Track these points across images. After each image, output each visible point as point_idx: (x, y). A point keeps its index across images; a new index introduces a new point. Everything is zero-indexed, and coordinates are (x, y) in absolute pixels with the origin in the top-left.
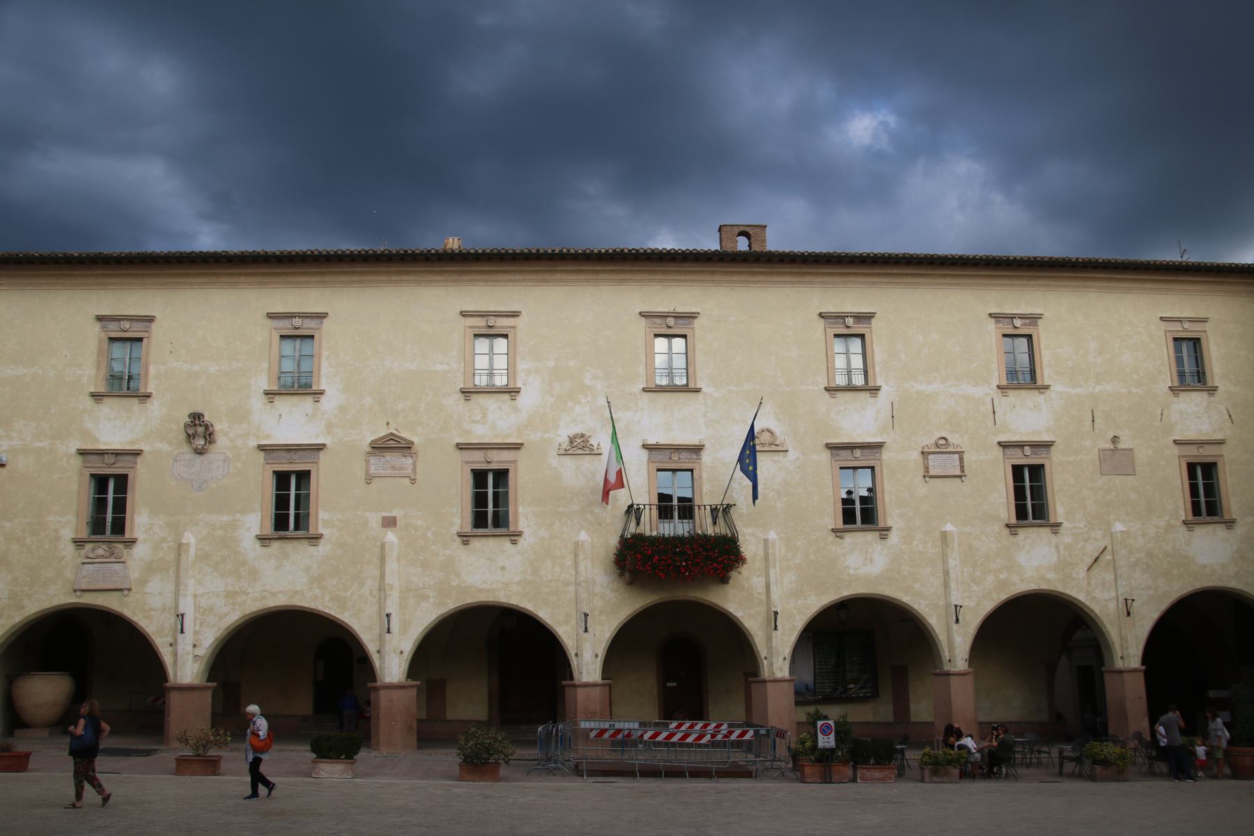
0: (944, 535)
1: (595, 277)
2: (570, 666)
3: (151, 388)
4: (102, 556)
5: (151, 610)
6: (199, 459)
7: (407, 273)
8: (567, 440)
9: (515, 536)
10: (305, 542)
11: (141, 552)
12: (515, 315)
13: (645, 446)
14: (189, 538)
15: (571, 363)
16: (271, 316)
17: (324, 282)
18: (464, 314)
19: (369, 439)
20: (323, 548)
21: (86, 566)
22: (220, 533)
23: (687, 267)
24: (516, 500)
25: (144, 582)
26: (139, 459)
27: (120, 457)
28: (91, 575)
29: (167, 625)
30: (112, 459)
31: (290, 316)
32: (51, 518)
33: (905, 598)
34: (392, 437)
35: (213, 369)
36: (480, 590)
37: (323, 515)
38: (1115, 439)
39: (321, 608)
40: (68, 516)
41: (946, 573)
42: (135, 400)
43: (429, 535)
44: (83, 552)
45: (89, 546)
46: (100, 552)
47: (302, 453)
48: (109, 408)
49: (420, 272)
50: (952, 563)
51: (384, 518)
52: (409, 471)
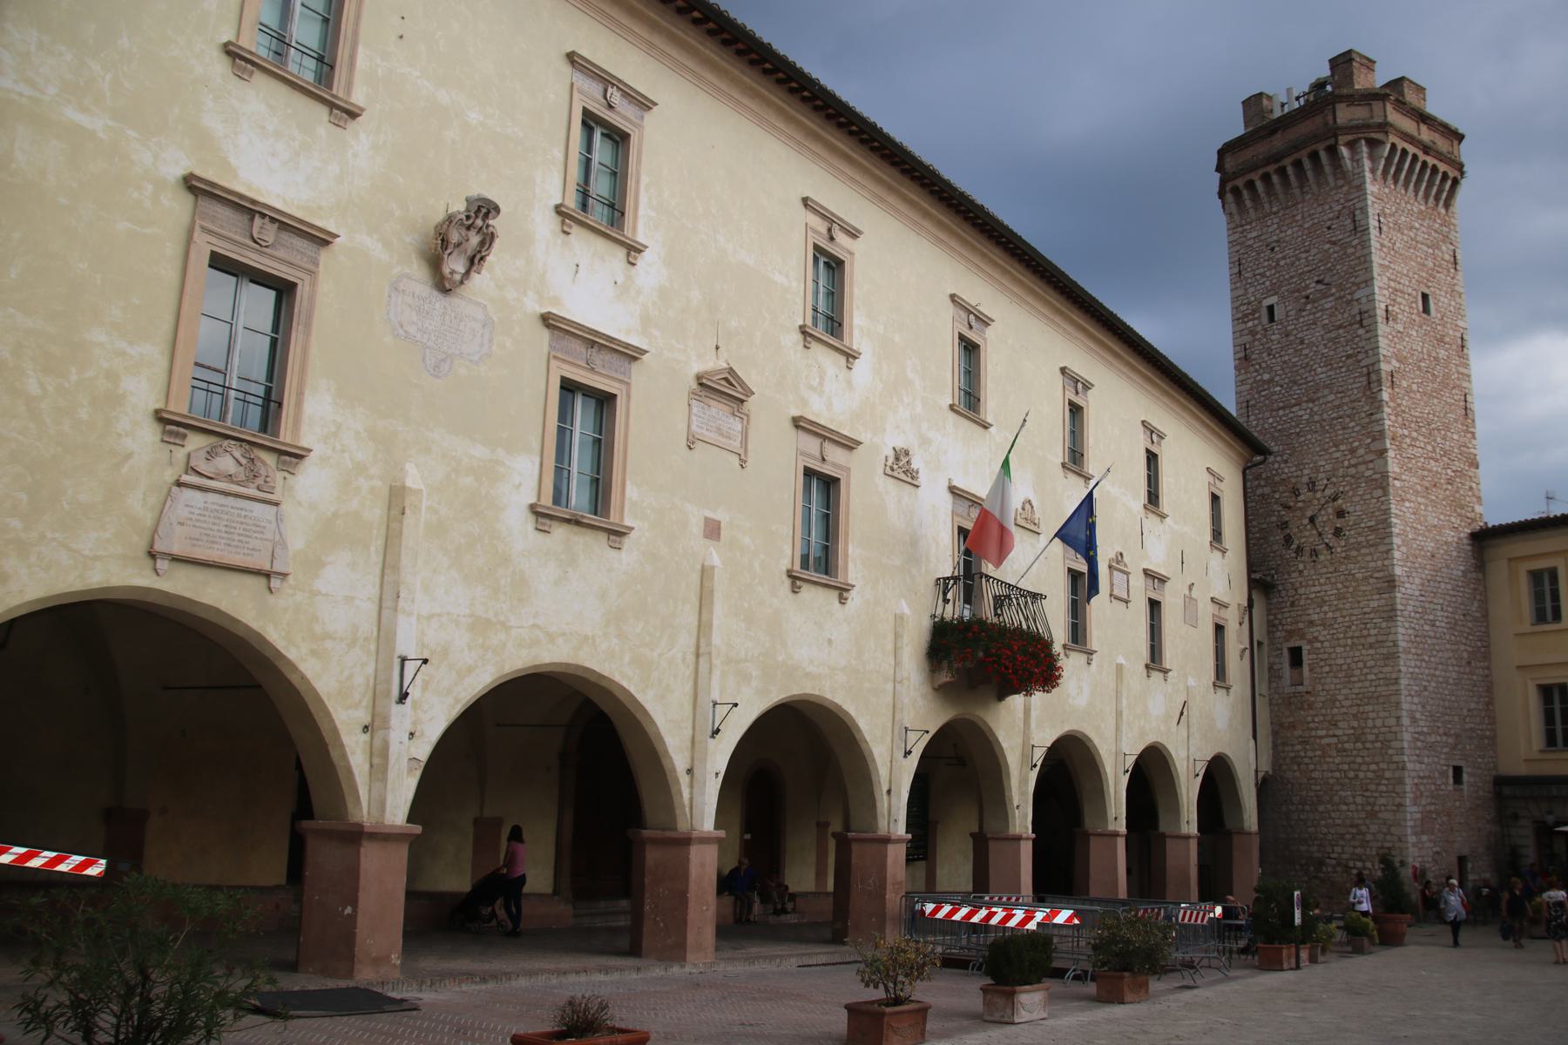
0: (1119, 668)
1: (917, 217)
2: (874, 806)
3: (358, 97)
4: (230, 478)
5: (328, 636)
6: (439, 302)
7: (755, 95)
8: (891, 454)
9: (843, 591)
10: (603, 537)
11: (309, 488)
12: (853, 234)
13: (954, 491)
14: (413, 478)
15: (897, 338)
16: (572, 58)
17: (651, 45)
18: (806, 201)
19: (697, 367)
20: (628, 557)
21: (188, 494)
22: (468, 480)
23: (996, 254)
24: (847, 534)
25: (315, 565)
26: (324, 255)
27: (286, 237)
28: (196, 520)
29: (359, 680)
30: (270, 234)
31: (606, 80)
32: (98, 336)
33: (1096, 741)
34: (731, 377)
35: (474, 117)
36: (807, 675)
37: (632, 492)
38: (1191, 586)
39: (617, 678)
40: (135, 345)
41: (1119, 714)
42: (323, 111)
43: (756, 565)
44: (180, 454)
45: (195, 442)
46: (226, 463)
47: (608, 357)
48: (260, 99)
49: (769, 104)
50: (1124, 702)
51: (707, 520)
52: (736, 444)
